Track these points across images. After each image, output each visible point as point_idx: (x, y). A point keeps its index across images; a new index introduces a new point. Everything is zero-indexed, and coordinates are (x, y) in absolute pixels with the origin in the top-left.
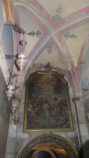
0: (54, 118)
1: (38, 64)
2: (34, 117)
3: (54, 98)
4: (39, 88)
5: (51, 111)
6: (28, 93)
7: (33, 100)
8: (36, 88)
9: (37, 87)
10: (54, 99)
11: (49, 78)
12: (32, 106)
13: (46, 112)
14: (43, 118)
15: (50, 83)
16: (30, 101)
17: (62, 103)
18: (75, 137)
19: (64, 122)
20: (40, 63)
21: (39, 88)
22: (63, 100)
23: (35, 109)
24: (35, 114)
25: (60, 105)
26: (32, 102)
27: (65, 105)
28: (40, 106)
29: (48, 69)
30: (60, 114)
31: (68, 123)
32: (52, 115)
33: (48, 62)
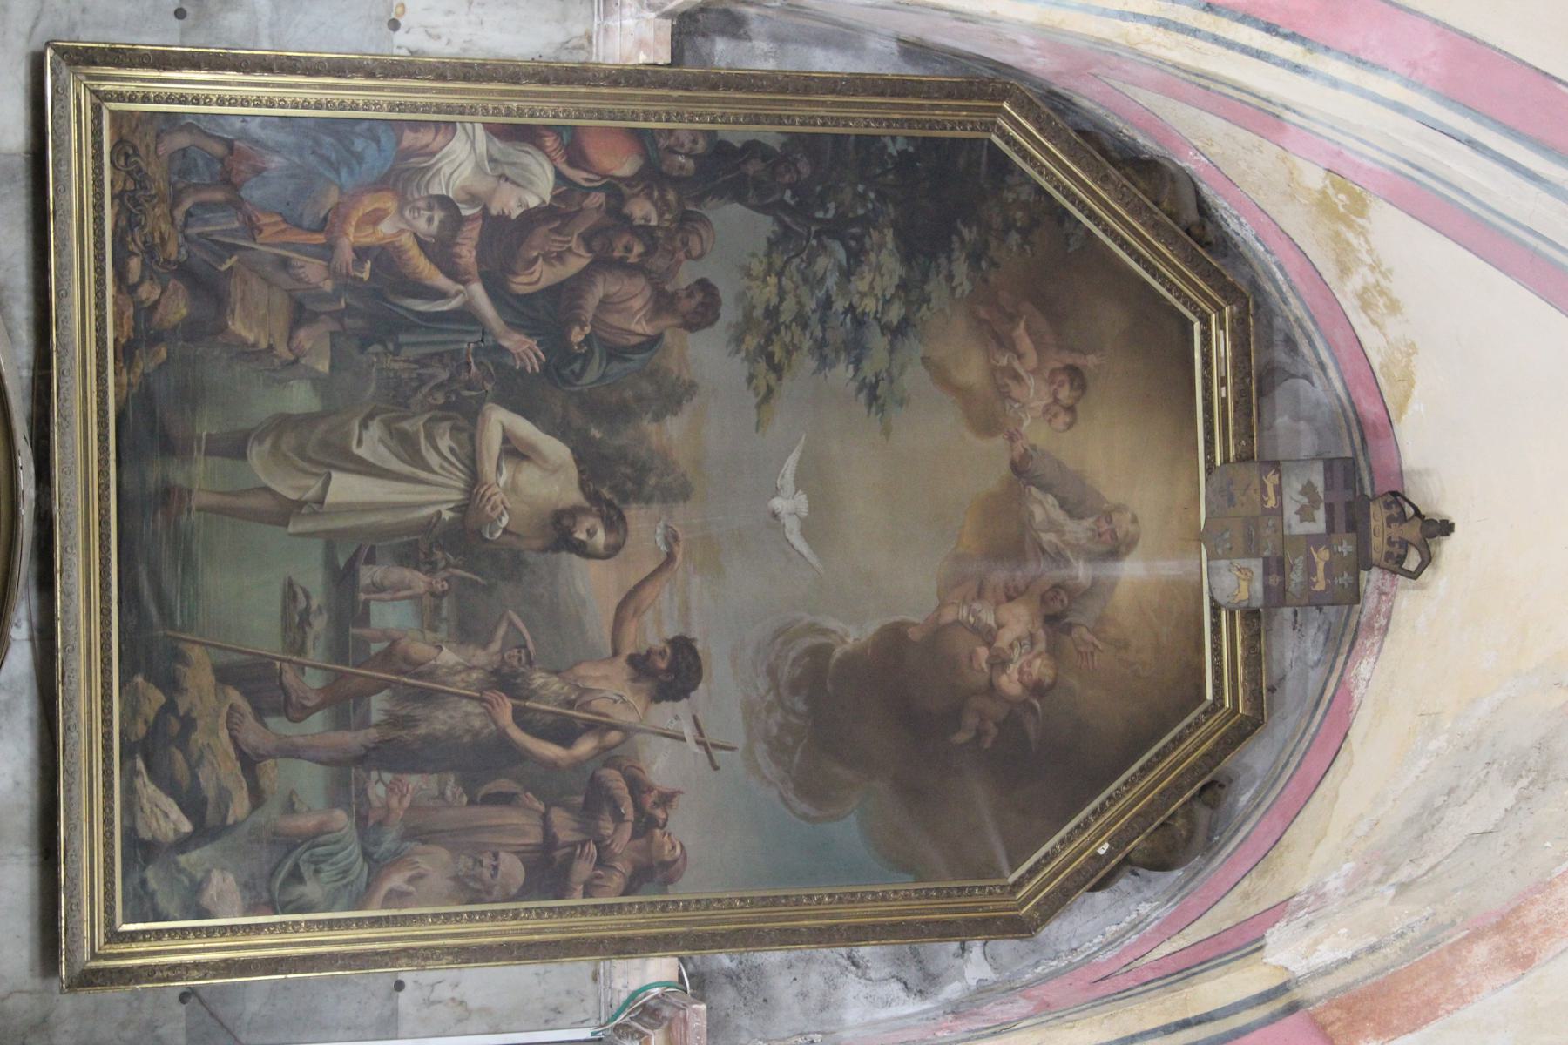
0: (305, 620)
1: (1394, 307)
2: (327, 252)
3: (695, 633)
4: (878, 343)
5: (432, 568)
6: (769, 134)
7: (644, 232)
8: (889, 283)
9: (895, 314)
10: (670, 632)
11: (1116, 550)
12: (533, 202)
13: (417, 459)
14: (310, 419)
15: (1000, 576)
16: (625, 166)
17: (596, 800)
19: (240, 806)
20: (1411, 350)
21: (878, 343)
22: (646, 825)
23: (467, 253)
24: (384, 258)
25: (550, 750)
26: (598, 199)
27: (549, 841)
28: (522, 348)
29: (1298, 528)
30: (373, 734)
31: (223, 884)
32: (367, 574)
33: (1446, 528)
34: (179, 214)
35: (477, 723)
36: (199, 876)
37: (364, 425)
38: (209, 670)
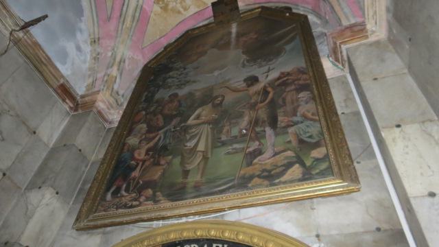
2: (144, 161)
3: (243, 79)
18: (378, 229)
25: (271, 95)
34: (126, 194)
35: (264, 109)
36: (313, 160)
37: (187, 146)
38: (248, 168)
